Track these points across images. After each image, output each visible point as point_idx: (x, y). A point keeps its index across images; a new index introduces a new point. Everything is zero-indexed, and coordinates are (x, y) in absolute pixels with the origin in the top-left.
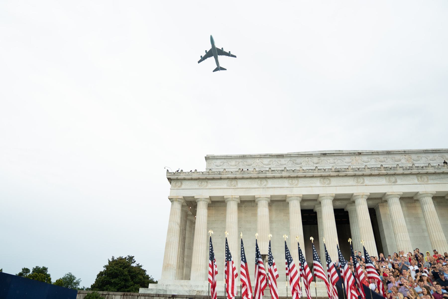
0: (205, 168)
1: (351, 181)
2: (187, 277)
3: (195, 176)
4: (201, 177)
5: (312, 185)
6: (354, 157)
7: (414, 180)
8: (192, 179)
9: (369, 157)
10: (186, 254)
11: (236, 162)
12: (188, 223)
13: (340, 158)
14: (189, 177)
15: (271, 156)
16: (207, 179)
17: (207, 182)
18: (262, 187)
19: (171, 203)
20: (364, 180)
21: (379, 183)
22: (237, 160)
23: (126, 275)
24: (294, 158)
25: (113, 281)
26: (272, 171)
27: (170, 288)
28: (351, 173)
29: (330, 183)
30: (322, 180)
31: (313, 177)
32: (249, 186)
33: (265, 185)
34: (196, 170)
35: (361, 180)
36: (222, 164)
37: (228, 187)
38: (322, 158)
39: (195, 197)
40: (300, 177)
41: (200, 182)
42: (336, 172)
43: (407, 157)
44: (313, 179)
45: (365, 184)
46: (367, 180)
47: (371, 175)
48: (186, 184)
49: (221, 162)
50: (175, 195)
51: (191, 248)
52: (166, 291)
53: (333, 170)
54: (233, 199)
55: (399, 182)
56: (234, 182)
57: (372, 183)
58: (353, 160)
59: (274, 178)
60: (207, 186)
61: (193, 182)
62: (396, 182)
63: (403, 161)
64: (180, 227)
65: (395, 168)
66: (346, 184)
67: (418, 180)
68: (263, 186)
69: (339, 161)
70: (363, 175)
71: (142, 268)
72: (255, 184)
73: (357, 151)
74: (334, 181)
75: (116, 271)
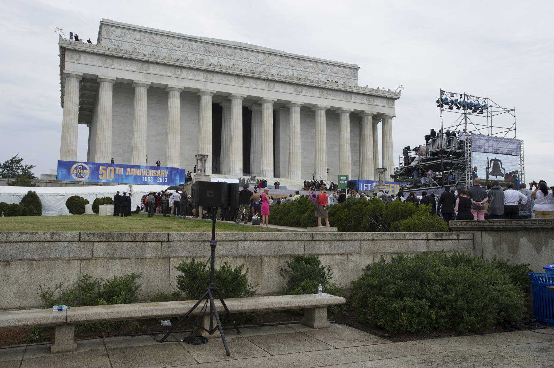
1: (263, 85)
4: (106, 52)
5: (227, 83)
7: (316, 93)
9: (282, 58)
11: (141, 36)
16: (113, 57)
17: (113, 61)
18: (175, 76)
20: (274, 85)
21: (287, 91)
22: (142, 34)
24: (207, 45)
29: (243, 84)
30: (236, 78)
31: (229, 74)
33: (179, 75)
35: (272, 85)
36: (123, 34)
37: (138, 71)
38: (236, 51)
39: (99, 77)
41: (104, 59)
44: (228, 76)
45: (274, 90)
46: (277, 87)
47: (282, 82)
49: (122, 32)
50: (72, 70)
56: (145, 66)
57: (281, 90)
59: (189, 68)
60: (112, 64)
62: (302, 92)
63: (311, 69)
66: (258, 87)
69: (253, 57)
70: (275, 81)
72: (168, 72)
73: (271, 49)
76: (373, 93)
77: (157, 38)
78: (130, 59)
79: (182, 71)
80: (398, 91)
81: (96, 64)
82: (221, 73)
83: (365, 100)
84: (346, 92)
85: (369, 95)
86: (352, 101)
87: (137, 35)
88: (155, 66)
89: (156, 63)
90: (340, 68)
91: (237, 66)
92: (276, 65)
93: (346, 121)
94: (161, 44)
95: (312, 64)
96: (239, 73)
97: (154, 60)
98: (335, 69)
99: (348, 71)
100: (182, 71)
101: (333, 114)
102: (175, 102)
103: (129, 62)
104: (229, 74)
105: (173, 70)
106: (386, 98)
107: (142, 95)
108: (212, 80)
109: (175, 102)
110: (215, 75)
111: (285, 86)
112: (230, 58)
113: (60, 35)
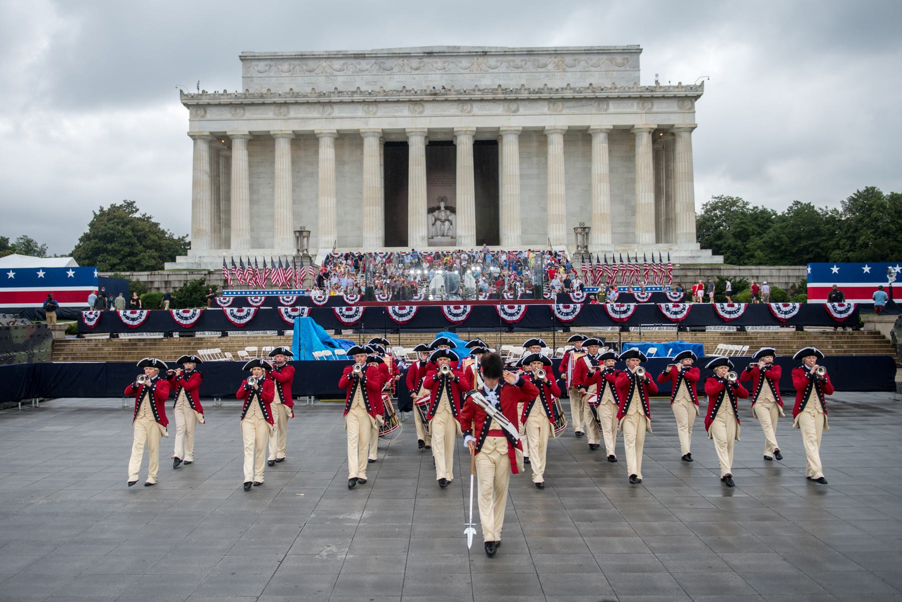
0: (240, 74)
1: (453, 109)
2: (227, 244)
3: (224, 100)
5: (397, 114)
6: (475, 59)
7: (544, 108)
8: (220, 105)
9: (500, 58)
10: (222, 207)
11: (290, 65)
12: (222, 161)
13: (454, 60)
14: (216, 102)
15: (345, 56)
17: (244, 110)
19: (192, 141)
20: (472, 107)
21: (494, 112)
22: (292, 62)
23: (129, 237)
25: (109, 247)
26: (339, 92)
27: (205, 260)
28: (453, 97)
29: (422, 112)
30: (412, 106)
31: (398, 102)
32: (305, 116)
33: (329, 114)
34: (225, 91)
35: (467, 107)
36: (267, 68)
37: (276, 117)
38: (426, 60)
39: (228, 133)
40: (380, 102)
42: (431, 95)
43: (557, 60)
46: (477, 109)
47: (482, 100)
48: (212, 113)
50: (197, 130)
51: (228, 200)
52: (200, 264)
53: (428, 92)
54: (284, 136)
55: (522, 110)
56: (284, 109)
58: (473, 64)
59: (341, 102)
60: (243, 115)
61: (223, 109)
62: (517, 110)
64: (211, 177)
65: (517, 91)
67: (549, 108)
68: (326, 115)
69: (451, 66)
70: (471, 100)
71: (153, 220)
72: (315, 112)
74: (429, 109)
75: (112, 232)
76: (648, 94)
77: (312, 64)
78: (264, 104)
79: (332, 108)
80: (698, 84)
81: (224, 117)
82: (387, 102)
83: (635, 107)
84: (596, 99)
85: (641, 98)
86: (609, 111)
87: (285, 66)
88: (297, 107)
89: (296, 103)
90: (605, 57)
91: (408, 88)
92: (490, 71)
93: (600, 146)
94: (316, 71)
95: (553, 59)
96: (413, 98)
97: (292, 100)
98: (595, 59)
99: (619, 59)
100: (332, 108)
101: (580, 138)
102: (327, 152)
103: (263, 108)
104: (398, 102)
105: (321, 108)
106: (675, 97)
107: (283, 150)
108: (375, 113)
109: (327, 152)
110: (380, 106)
111: (490, 105)
112: (417, 72)
113: (181, 91)
